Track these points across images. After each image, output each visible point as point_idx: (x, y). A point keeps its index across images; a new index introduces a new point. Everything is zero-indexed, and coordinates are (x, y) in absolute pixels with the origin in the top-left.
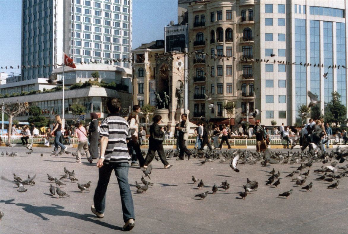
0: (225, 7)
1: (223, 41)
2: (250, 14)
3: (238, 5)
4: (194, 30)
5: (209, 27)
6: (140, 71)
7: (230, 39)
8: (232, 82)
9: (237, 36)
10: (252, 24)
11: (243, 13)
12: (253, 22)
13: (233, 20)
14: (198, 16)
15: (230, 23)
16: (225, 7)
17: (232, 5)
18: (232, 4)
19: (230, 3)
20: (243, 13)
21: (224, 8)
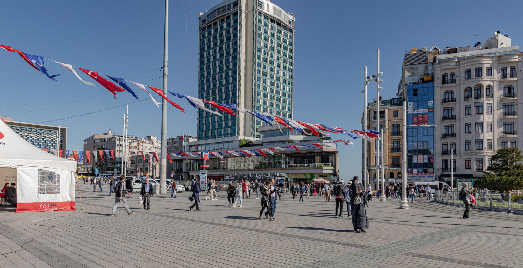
0: (486, 63)
1: (483, 98)
3: (499, 62)
7: (490, 95)
8: (492, 138)
9: (498, 93)
10: (515, 81)
11: (504, 70)
12: (516, 79)
13: (494, 76)
15: (491, 80)
16: (486, 63)
17: (491, 62)
19: (490, 60)
20: (504, 70)
21: (484, 64)
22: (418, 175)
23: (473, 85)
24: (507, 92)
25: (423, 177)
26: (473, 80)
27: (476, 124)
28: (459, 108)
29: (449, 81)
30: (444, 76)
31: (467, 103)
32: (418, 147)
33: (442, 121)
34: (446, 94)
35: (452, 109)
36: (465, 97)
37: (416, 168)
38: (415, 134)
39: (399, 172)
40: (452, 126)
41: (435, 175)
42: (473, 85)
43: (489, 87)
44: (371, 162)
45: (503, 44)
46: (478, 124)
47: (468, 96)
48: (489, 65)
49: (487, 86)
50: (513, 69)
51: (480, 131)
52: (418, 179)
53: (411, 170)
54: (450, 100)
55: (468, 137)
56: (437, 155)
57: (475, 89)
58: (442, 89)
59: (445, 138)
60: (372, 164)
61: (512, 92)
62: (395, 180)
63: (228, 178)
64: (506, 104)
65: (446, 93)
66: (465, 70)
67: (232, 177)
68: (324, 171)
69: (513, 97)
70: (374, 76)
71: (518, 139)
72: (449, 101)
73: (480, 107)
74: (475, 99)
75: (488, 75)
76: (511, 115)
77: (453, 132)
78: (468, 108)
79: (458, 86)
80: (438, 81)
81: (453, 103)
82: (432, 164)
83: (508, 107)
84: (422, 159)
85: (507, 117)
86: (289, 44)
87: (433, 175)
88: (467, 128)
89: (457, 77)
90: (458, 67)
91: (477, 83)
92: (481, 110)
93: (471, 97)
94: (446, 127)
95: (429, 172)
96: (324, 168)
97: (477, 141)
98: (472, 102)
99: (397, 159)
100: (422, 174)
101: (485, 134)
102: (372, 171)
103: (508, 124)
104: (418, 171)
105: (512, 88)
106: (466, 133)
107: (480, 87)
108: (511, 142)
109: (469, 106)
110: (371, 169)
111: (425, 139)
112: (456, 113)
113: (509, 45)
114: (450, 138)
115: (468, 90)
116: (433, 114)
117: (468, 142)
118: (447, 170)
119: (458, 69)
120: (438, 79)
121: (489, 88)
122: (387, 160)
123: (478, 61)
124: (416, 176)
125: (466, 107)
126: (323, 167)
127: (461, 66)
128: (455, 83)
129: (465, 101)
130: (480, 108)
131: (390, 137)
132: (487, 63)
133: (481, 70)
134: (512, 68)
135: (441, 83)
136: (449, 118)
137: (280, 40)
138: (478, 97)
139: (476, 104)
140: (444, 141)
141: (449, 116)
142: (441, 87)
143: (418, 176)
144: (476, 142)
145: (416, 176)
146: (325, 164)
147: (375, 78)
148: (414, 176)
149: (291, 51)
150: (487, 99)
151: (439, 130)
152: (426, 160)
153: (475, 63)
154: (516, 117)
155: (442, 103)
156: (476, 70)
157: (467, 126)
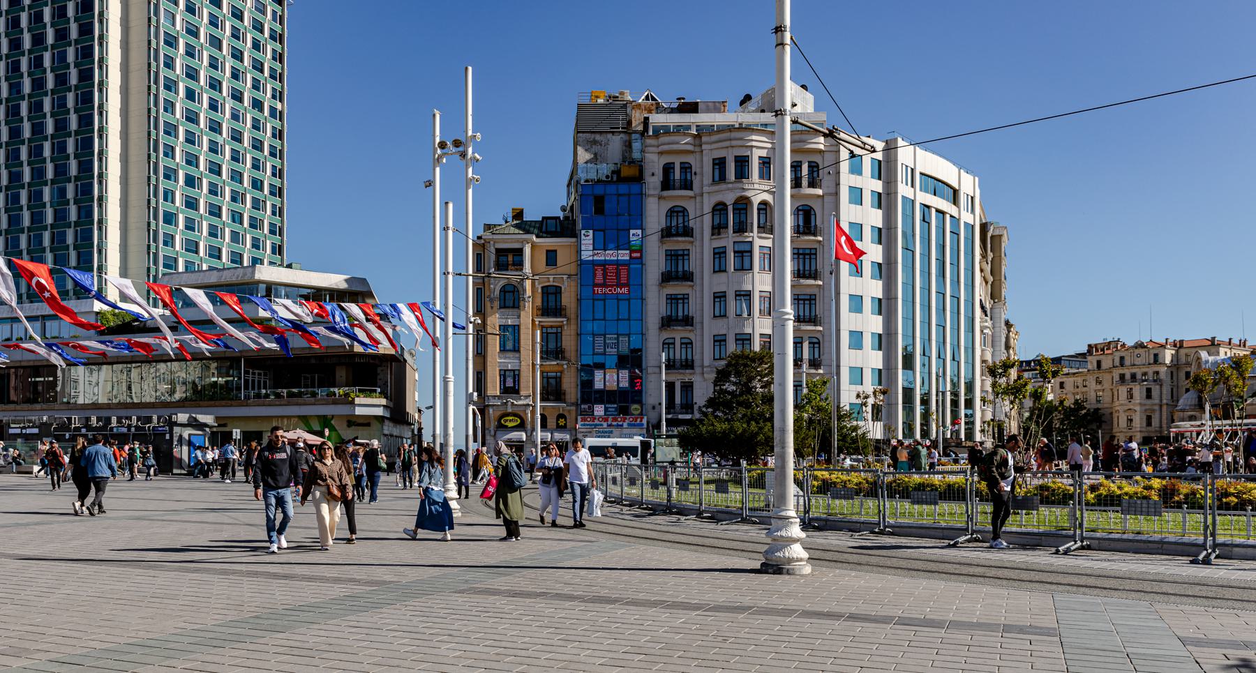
1: (752, 232)
2: (793, 173)
4: (660, 198)
5: (709, 193)
6: (548, 294)
10: (819, 196)
12: (820, 192)
14: (674, 163)
17: (769, 146)
18: (771, 143)
19: (767, 140)
21: (754, 149)
22: (606, 420)
23: (729, 198)
24: (801, 223)
25: (618, 425)
26: (730, 186)
27: (736, 295)
28: (702, 249)
29: (677, 184)
30: (668, 169)
31: (718, 243)
32: (605, 349)
33: (663, 284)
34: (671, 216)
35: (685, 255)
36: (713, 228)
37: (600, 402)
38: (599, 315)
39: (561, 412)
40: (685, 298)
41: (645, 421)
42: (729, 198)
43: (763, 207)
44: (489, 385)
45: (796, 105)
46: (740, 295)
47: (719, 224)
48: (764, 153)
49: (759, 204)
50: (814, 167)
51: (745, 315)
52: (606, 432)
53: (589, 408)
54: (681, 230)
55: (720, 327)
56: (650, 370)
57: (734, 209)
58: (662, 202)
59: (669, 326)
60: (490, 392)
61: (813, 224)
62: (549, 435)
63: (18, 431)
64: (801, 251)
65: (672, 212)
66: (714, 159)
67: (33, 427)
68: (359, 411)
69: (815, 235)
70: (457, 143)
71: (823, 336)
72: (678, 235)
73: (745, 254)
74: (734, 232)
75: (761, 177)
76: (809, 277)
77: (686, 313)
78: (719, 254)
79: (697, 198)
80: (653, 181)
81: (687, 239)
82: (640, 392)
83: (804, 259)
84: (616, 379)
85: (803, 281)
86: (272, 37)
87: (641, 421)
88: (717, 305)
89: (695, 174)
90: (697, 149)
91: (739, 194)
92: (747, 260)
93: (727, 227)
94: (672, 299)
95: (634, 415)
96: (357, 401)
97: (738, 337)
98: (728, 240)
99: (556, 378)
100: (615, 420)
101: (757, 321)
102: (491, 411)
103: (804, 300)
104: (606, 410)
105: (813, 213)
106: (715, 316)
107: (746, 204)
108: (810, 343)
109: (721, 250)
110: (488, 406)
111: (623, 327)
112: (693, 265)
113: (810, 109)
114: (679, 328)
115: (720, 208)
116: (642, 264)
117: (719, 338)
118: (674, 408)
119: (698, 156)
120: (653, 174)
121: (766, 209)
122: (529, 382)
123: (741, 139)
124: (602, 425)
125: (717, 251)
126: (353, 399)
127: (704, 147)
128: (691, 189)
129: (714, 237)
130: (744, 255)
131: (537, 320)
132: (759, 147)
133: (748, 161)
134: (813, 164)
135: (659, 185)
136: (677, 278)
137: (241, 19)
138: (742, 228)
139: (736, 246)
140: (666, 335)
141: (677, 272)
142: (660, 198)
143: (605, 425)
144: (736, 340)
145: (602, 425)
146: (360, 391)
147: (461, 149)
148: (596, 425)
149: (279, 57)
150: (760, 235)
151: (655, 304)
152: (625, 384)
153: (734, 143)
154: (820, 283)
155: (663, 237)
156: (736, 162)
157: (718, 300)
